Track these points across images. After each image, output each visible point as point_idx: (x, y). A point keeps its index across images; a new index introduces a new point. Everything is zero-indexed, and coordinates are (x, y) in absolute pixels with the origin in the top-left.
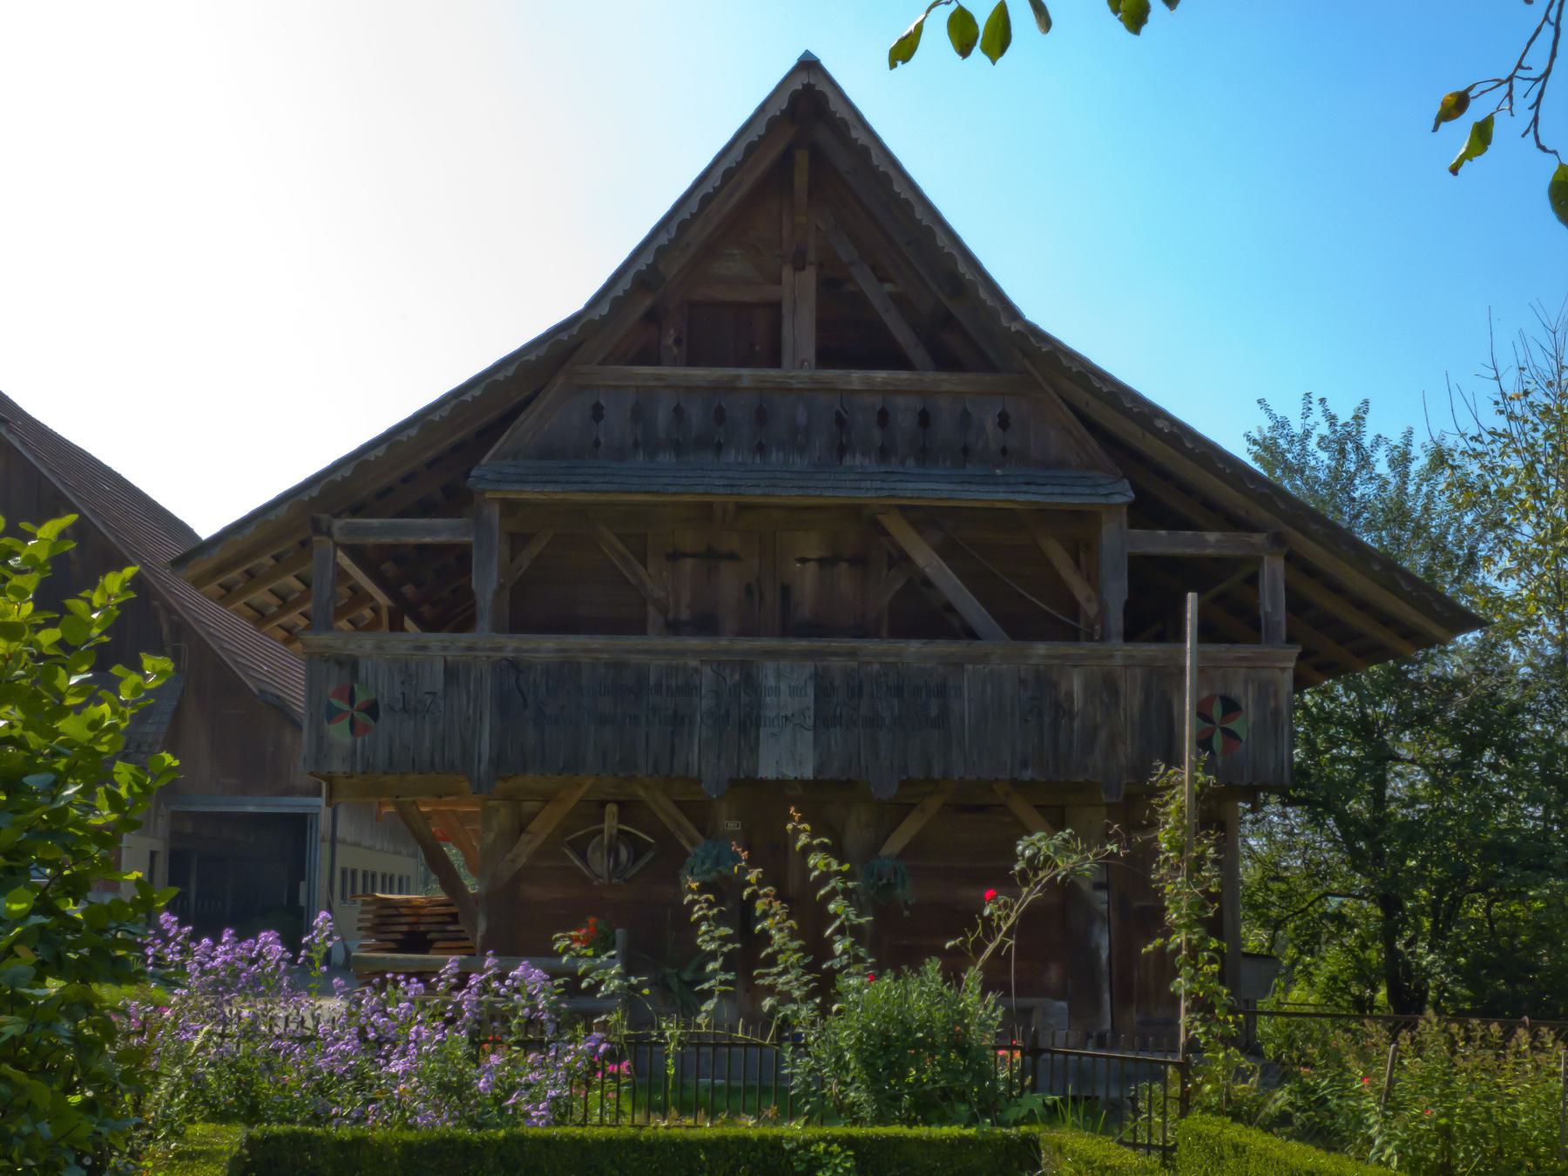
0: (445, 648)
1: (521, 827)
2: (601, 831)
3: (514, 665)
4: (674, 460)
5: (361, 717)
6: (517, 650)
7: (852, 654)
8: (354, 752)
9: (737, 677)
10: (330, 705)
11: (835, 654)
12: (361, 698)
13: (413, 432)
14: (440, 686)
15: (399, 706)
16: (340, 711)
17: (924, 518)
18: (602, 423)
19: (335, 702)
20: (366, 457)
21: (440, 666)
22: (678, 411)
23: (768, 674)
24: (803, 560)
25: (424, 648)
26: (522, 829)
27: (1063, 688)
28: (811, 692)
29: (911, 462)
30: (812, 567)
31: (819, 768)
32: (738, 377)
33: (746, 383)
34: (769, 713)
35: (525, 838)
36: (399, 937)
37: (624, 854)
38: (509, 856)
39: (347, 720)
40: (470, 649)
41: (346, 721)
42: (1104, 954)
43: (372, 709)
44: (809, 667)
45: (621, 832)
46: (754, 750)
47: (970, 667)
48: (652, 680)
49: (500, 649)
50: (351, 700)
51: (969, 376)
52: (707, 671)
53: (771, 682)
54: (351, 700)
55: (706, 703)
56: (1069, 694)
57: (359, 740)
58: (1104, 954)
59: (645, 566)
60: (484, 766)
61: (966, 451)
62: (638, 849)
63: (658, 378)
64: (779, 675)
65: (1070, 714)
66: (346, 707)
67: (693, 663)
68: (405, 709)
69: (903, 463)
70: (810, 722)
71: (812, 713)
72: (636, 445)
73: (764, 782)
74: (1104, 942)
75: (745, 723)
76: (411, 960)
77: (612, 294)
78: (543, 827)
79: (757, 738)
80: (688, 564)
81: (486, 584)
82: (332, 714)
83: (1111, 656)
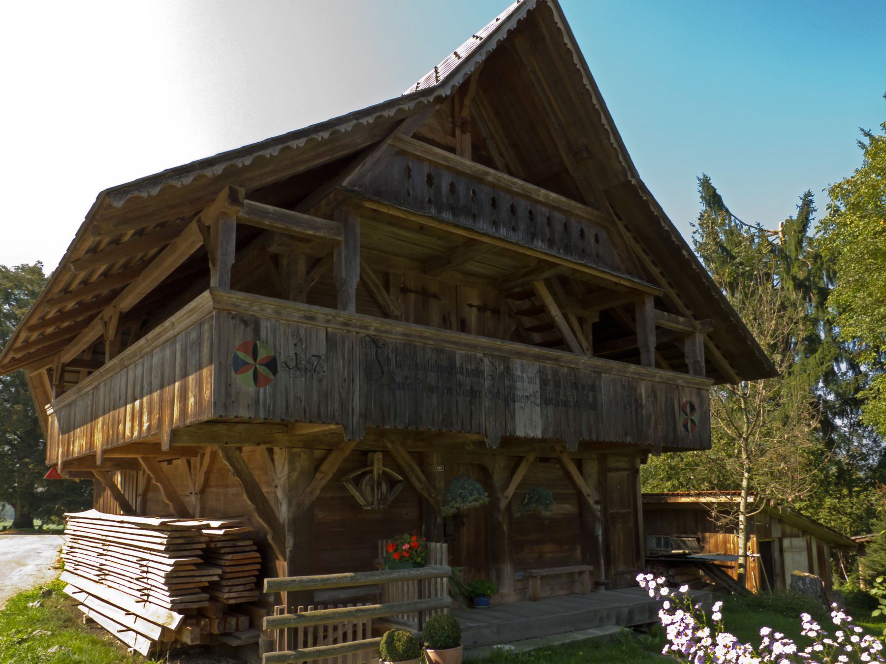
0: (328, 321)
1: (317, 467)
2: (371, 472)
3: (374, 341)
4: (451, 218)
5: (262, 370)
6: (377, 330)
7: (556, 360)
8: (257, 401)
9: (502, 367)
10: (236, 357)
11: (549, 359)
12: (262, 354)
13: (301, 142)
14: (323, 351)
15: (292, 364)
16: (245, 363)
17: (564, 284)
18: (411, 180)
19: (241, 355)
20: (290, 144)
21: (323, 335)
22: (453, 188)
23: (517, 365)
24: (470, 306)
25: (312, 318)
26: (317, 468)
27: (639, 392)
28: (538, 381)
29: (562, 251)
30: (474, 311)
31: (543, 432)
32: (487, 173)
33: (490, 179)
34: (519, 393)
35: (318, 476)
36: (200, 553)
37: (384, 487)
38: (308, 489)
39: (251, 372)
40: (345, 324)
41: (250, 373)
42: (600, 538)
43: (272, 365)
44: (537, 365)
45: (384, 472)
46: (513, 417)
47: (603, 375)
48: (458, 365)
49: (366, 328)
50: (255, 358)
51: (589, 209)
52: (487, 361)
53: (519, 373)
54: (255, 358)
55: (487, 383)
56: (641, 394)
57: (262, 390)
58: (600, 538)
59: (389, 293)
60: (356, 417)
61: (583, 251)
62: (392, 483)
63: (446, 159)
64: (523, 370)
65: (641, 406)
66: (250, 360)
67: (480, 355)
68: (297, 367)
69: (559, 250)
70: (538, 401)
71: (538, 395)
72: (430, 201)
73: (518, 438)
74: (600, 533)
75: (506, 399)
76: (328, 579)
77: (451, 83)
78: (330, 467)
79: (514, 410)
80: (412, 297)
81: (350, 274)
82: (239, 366)
83: (655, 376)
